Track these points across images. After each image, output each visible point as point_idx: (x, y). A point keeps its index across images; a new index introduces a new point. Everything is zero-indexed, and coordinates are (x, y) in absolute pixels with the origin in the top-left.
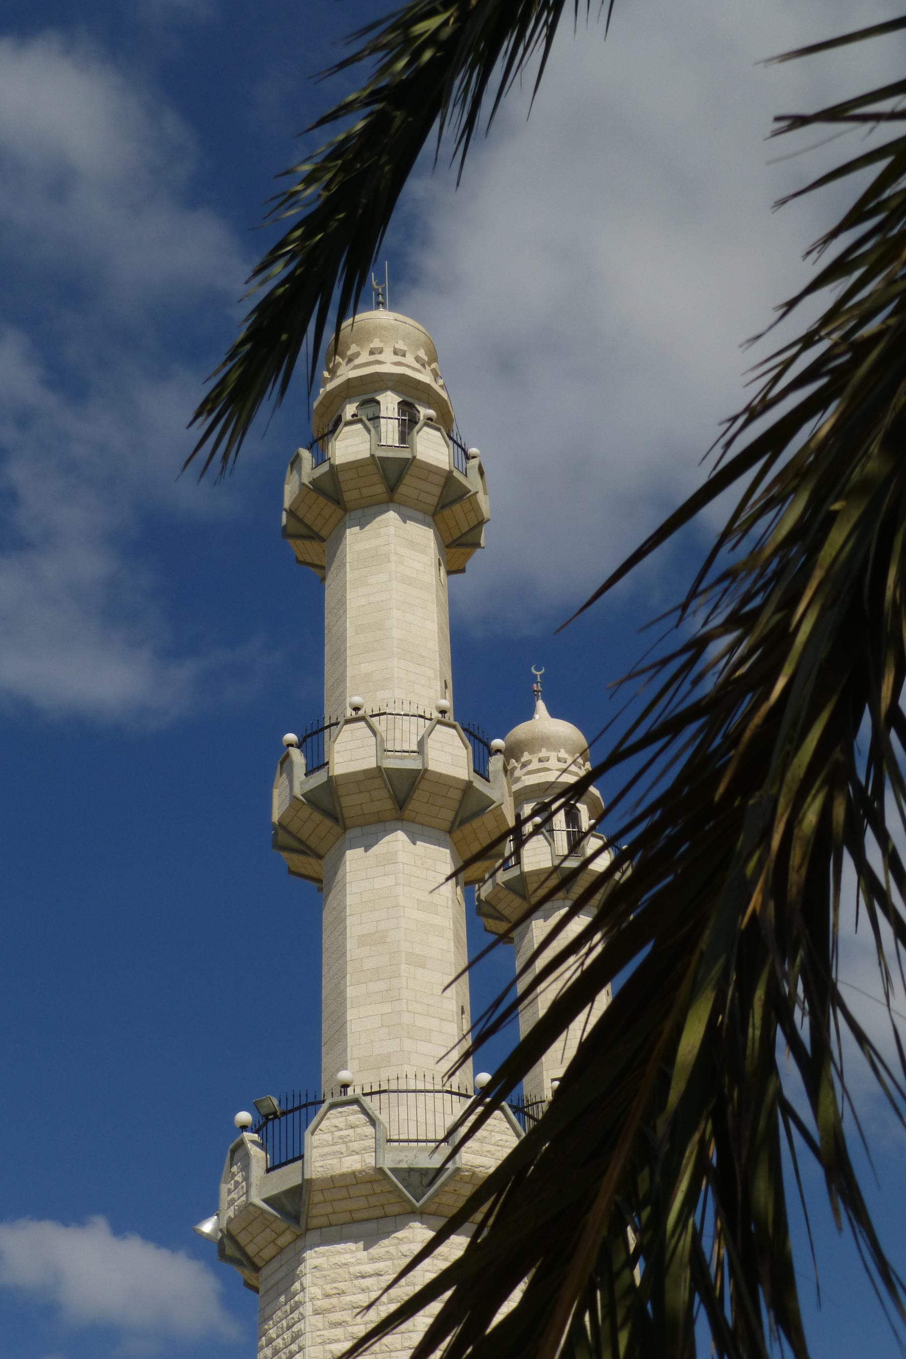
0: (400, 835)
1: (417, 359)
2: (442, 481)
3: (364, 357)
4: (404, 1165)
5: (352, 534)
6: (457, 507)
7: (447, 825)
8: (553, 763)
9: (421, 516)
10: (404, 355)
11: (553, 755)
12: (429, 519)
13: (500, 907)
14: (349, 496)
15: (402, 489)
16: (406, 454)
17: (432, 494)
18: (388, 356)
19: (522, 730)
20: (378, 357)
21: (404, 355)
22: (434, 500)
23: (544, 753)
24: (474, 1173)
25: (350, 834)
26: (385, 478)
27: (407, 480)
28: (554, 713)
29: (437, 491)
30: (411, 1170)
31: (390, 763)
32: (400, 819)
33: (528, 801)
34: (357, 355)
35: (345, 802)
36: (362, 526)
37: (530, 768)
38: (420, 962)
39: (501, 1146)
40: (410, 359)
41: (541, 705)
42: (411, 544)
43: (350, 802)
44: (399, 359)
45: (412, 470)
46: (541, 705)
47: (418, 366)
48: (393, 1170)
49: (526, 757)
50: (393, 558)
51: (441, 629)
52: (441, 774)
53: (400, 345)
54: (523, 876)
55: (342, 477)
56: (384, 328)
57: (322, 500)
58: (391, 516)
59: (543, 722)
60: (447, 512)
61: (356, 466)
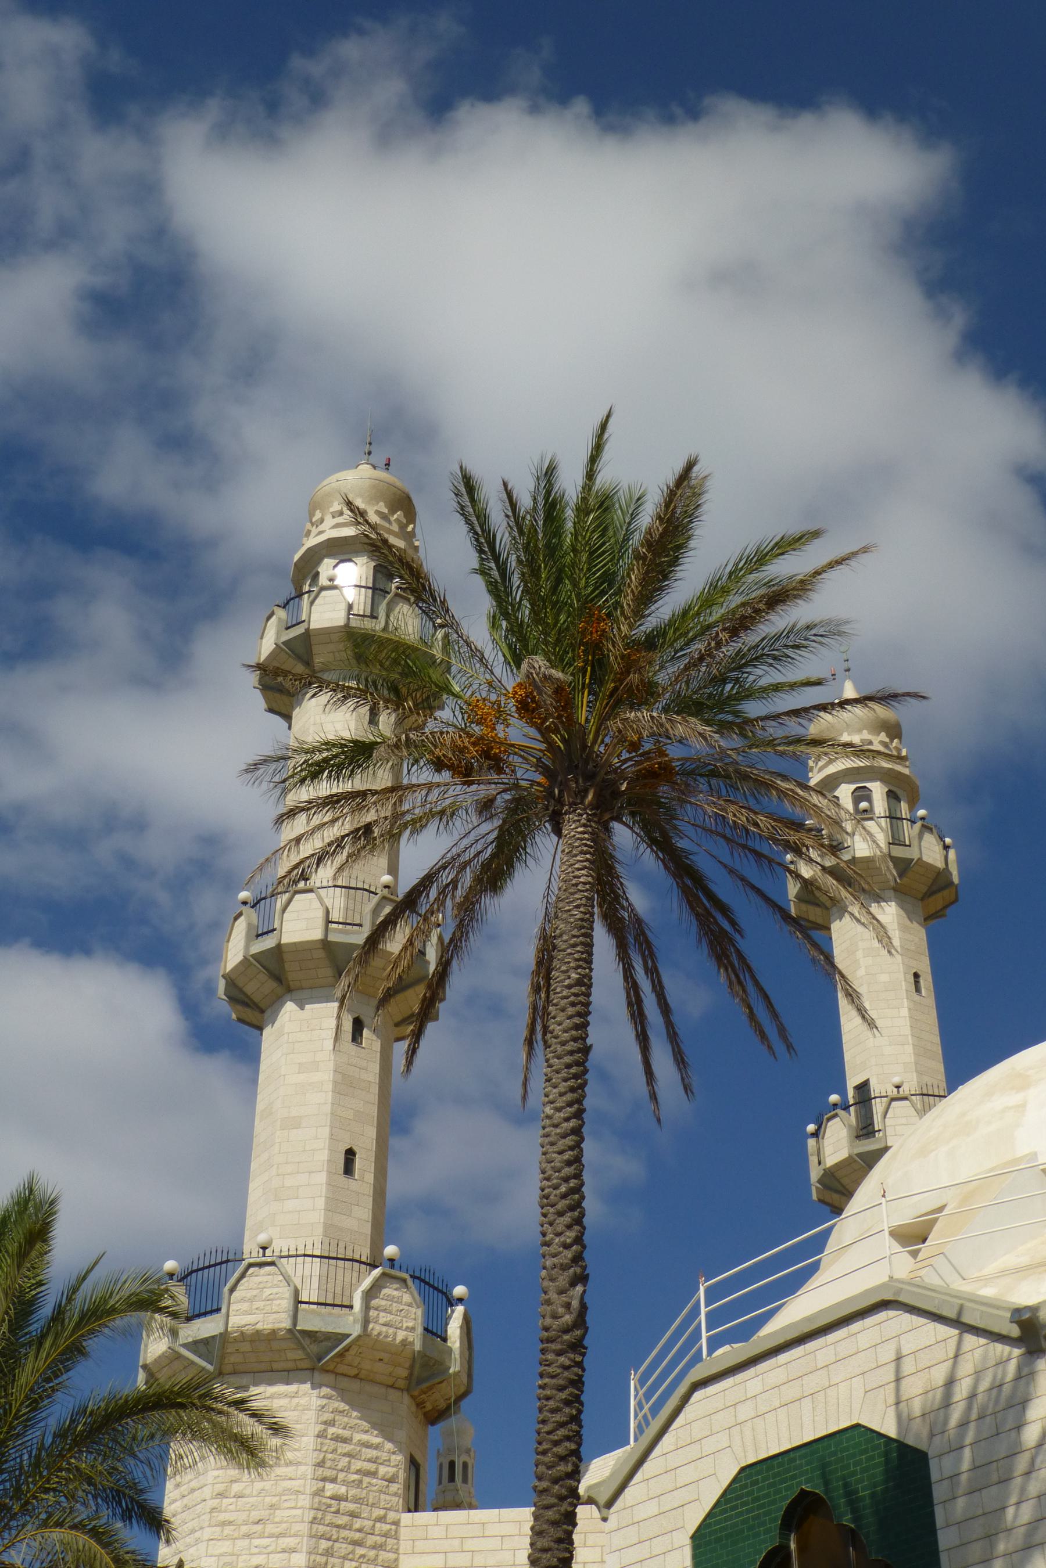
0: (290, 1007)
4: (190, 1340)
16: (300, 630)
18: (329, 521)
20: (321, 528)
24: (242, 1333)
26: (299, 657)
27: (315, 649)
30: (195, 1343)
32: (289, 990)
38: (294, 1123)
39: (272, 1300)
43: (250, 989)
45: (314, 640)
52: (295, 943)
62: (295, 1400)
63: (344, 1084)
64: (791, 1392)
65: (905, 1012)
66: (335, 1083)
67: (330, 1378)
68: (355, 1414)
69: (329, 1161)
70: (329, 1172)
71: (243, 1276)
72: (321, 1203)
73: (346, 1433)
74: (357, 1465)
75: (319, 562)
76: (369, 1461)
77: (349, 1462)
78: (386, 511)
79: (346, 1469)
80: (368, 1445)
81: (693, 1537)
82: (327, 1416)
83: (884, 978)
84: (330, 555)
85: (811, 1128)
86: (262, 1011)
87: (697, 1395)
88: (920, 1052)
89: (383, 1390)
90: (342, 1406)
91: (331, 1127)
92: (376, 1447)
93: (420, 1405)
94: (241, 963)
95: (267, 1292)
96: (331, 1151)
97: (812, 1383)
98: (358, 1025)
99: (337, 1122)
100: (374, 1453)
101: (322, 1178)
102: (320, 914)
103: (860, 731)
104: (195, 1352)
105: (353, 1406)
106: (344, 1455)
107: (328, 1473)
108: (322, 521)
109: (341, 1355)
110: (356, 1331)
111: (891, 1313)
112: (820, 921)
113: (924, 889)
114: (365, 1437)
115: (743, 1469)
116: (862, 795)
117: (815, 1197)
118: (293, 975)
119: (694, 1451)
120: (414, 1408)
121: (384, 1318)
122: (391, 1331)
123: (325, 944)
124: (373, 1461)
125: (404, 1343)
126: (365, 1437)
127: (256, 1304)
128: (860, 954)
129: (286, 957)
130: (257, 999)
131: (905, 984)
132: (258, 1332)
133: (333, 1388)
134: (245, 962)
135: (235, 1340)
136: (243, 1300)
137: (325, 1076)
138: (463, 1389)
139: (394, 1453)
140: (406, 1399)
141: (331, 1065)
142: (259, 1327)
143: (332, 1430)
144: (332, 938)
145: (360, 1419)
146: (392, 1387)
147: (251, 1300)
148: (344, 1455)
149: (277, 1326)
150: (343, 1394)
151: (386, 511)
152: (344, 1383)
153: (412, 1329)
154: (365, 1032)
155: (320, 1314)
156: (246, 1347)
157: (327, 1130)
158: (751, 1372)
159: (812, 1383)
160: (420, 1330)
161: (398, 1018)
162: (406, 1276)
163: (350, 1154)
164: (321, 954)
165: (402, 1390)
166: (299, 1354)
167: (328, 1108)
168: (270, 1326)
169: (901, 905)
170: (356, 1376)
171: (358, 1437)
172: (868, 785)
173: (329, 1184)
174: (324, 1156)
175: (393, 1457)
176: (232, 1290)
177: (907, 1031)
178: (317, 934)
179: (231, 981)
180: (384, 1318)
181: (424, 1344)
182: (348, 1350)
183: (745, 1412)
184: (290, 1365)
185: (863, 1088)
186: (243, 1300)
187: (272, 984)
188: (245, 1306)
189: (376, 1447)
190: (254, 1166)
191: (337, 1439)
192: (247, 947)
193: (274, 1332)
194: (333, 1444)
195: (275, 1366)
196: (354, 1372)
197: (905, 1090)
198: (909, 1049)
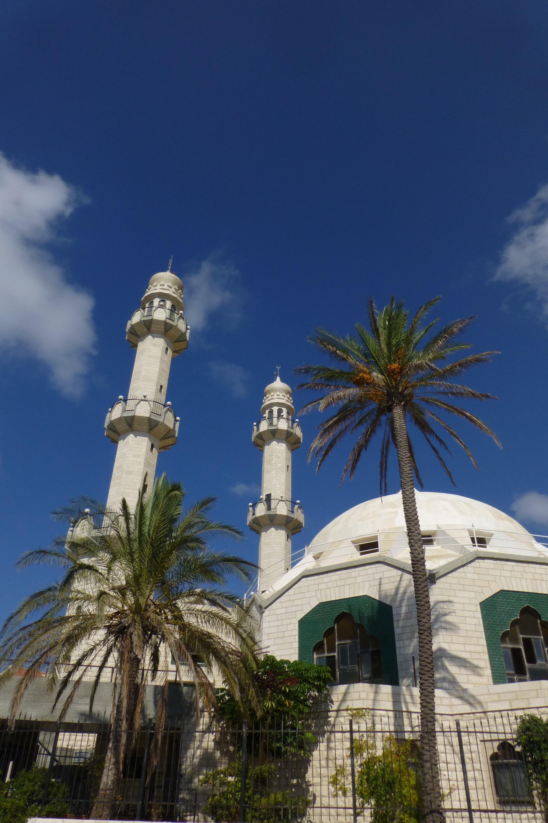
1: (168, 286)
3: (153, 288)
5: (140, 344)
6: (171, 331)
7: (147, 430)
8: (275, 396)
9: (160, 335)
10: (163, 285)
11: (275, 394)
12: (163, 336)
13: (258, 443)
14: (139, 333)
15: (152, 328)
16: (150, 318)
18: (159, 287)
19: (268, 387)
20: (156, 288)
21: (163, 285)
22: (163, 330)
23: (272, 394)
25: (120, 437)
26: (146, 326)
27: (153, 326)
28: (282, 380)
29: (163, 327)
31: (125, 415)
33: (267, 409)
34: (151, 288)
35: (117, 427)
36: (142, 341)
37: (269, 399)
40: (166, 287)
41: (278, 378)
42: (155, 345)
43: (118, 427)
44: (162, 287)
46: (278, 378)
47: (168, 288)
49: (268, 395)
50: (147, 350)
51: (161, 370)
53: (162, 283)
54: (260, 434)
55: (135, 328)
56: (159, 278)
57: (133, 336)
58: (150, 337)
59: (278, 384)
60: (168, 333)
61: (137, 324)
63: (147, 463)
64: (342, 583)
65: (284, 476)
75: (155, 298)
81: (299, 621)
83: (280, 465)
84: (158, 297)
85: (251, 504)
86: (119, 435)
88: (286, 488)
94: (119, 418)
97: (349, 581)
98: (152, 446)
103: (282, 392)
108: (156, 286)
111: (381, 565)
112: (260, 444)
113: (293, 442)
115: (320, 603)
116: (280, 411)
117: (248, 524)
118: (135, 425)
123: (149, 419)
128: (274, 457)
129: (135, 420)
130: (119, 431)
131: (285, 468)
134: (120, 418)
137: (142, 460)
141: (144, 457)
154: (154, 449)
158: (326, 575)
159: (349, 581)
164: (147, 421)
167: (142, 470)
169: (287, 445)
177: (284, 482)
178: (147, 415)
179: (112, 423)
183: (321, 587)
185: (269, 497)
187: (127, 427)
190: (112, 484)
192: (122, 414)
197: (284, 499)
198: (284, 487)
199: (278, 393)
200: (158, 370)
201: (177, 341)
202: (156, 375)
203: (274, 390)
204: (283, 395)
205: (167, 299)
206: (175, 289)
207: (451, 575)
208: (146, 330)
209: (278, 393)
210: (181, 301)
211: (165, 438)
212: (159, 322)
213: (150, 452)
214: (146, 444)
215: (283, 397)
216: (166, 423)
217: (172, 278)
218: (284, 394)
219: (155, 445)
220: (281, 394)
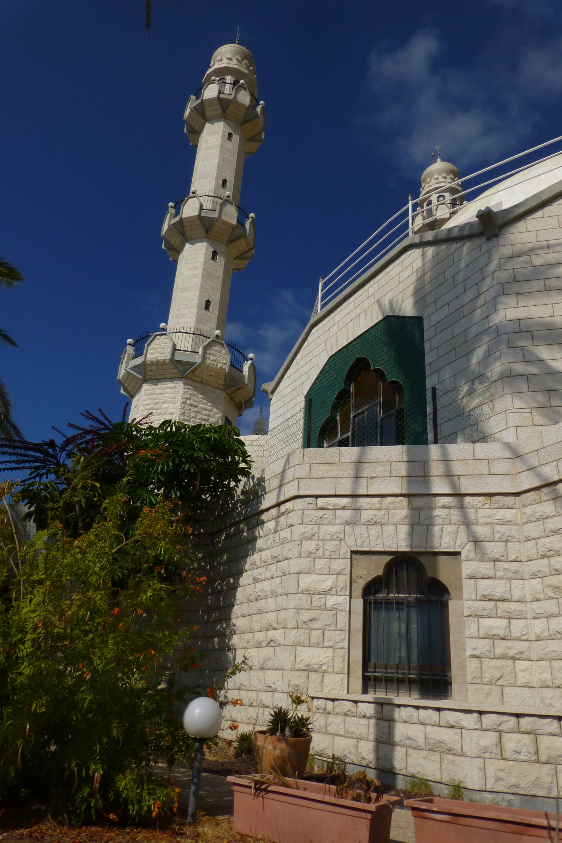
0: (188, 246)
2: (217, 102)
6: (230, 108)
15: (207, 114)
17: (218, 109)
22: (220, 111)
24: (152, 361)
29: (218, 107)
30: (135, 367)
38: (186, 290)
45: (205, 105)
48: (131, 369)
62: (174, 390)
63: (207, 275)
66: (203, 274)
67: (190, 381)
68: (200, 396)
69: (198, 304)
70: (198, 308)
71: (153, 339)
72: (194, 319)
73: (196, 404)
74: (199, 416)
76: (205, 415)
77: (196, 415)
78: (240, 59)
79: (195, 417)
80: (205, 409)
81: (306, 397)
82: (187, 396)
87: (314, 330)
89: (214, 389)
90: (194, 393)
91: (200, 291)
92: (209, 410)
93: (232, 399)
95: (163, 345)
96: (199, 300)
99: (203, 289)
100: (208, 413)
101: (195, 310)
102: (198, 206)
104: (135, 371)
105: (200, 393)
106: (194, 412)
107: (186, 418)
109: (193, 371)
110: (199, 361)
114: (204, 406)
115: (330, 358)
119: (310, 357)
120: (228, 399)
121: (212, 358)
122: (215, 363)
123: (200, 217)
124: (208, 415)
125: (221, 368)
126: (204, 406)
127: (158, 350)
129: (184, 224)
132: (158, 361)
133: (191, 386)
135: (149, 365)
136: (153, 349)
137: (199, 272)
138: (251, 395)
139: (217, 413)
140: (224, 393)
142: (159, 359)
143: (188, 402)
144: (203, 214)
145: (203, 398)
146: (218, 388)
147: (156, 349)
148: (194, 412)
149: (166, 358)
150: (195, 388)
151: (240, 59)
152: (195, 384)
153: (226, 364)
155: (184, 354)
156: (154, 368)
157: (198, 292)
158: (338, 310)
160: (228, 364)
161: (235, 256)
162: (223, 342)
163: (208, 303)
164: (198, 222)
165: (222, 390)
166: (175, 371)
167: (199, 284)
168: (163, 358)
170: (201, 382)
171: (200, 406)
172: (443, 194)
173: (198, 312)
174: (196, 301)
175: (216, 415)
176: (149, 345)
180: (212, 358)
181: (230, 370)
182: (196, 370)
183: (333, 331)
184: (173, 376)
186: (153, 349)
187: (181, 238)
188: (153, 351)
189: (209, 410)
191: (191, 405)
193: (164, 361)
194: (189, 407)
195: (167, 376)
196: (200, 380)
199: (436, 176)
200: (216, 161)
201: (245, 121)
202: (215, 168)
203: (431, 175)
204: (443, 177)
205: (227, 75)
206: (237, 59)
207: (539, 214)
208: (201, 119)
209: (436, 176)
210: (246, 71)
211: (232, 241)
212: (211, 100)
213: (211, 262)
214: (204, 251)
215: (443, 180)
216: (224, 218)
217: (233, 48)
218: (444, 175)
219: (219, 252)
220: (440, 177)
